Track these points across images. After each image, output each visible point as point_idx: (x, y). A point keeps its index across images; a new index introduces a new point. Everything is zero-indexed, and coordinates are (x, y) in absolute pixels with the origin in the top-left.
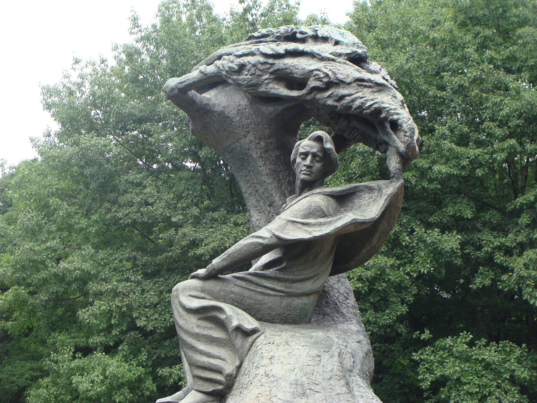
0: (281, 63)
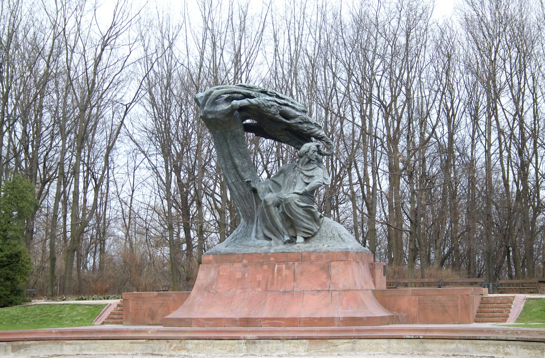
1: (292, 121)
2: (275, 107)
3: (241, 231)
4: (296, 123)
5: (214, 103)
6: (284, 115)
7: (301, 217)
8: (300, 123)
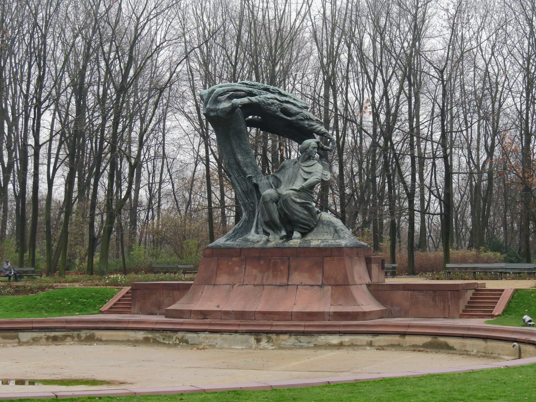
0: (285, 105)
1: (293, 118)
2: (276, 104)
3: (242, 225)
4: (297, 120)
5: (216, 101)
6: (285, 111)
7: (297, 213)
8: (301, 120)
